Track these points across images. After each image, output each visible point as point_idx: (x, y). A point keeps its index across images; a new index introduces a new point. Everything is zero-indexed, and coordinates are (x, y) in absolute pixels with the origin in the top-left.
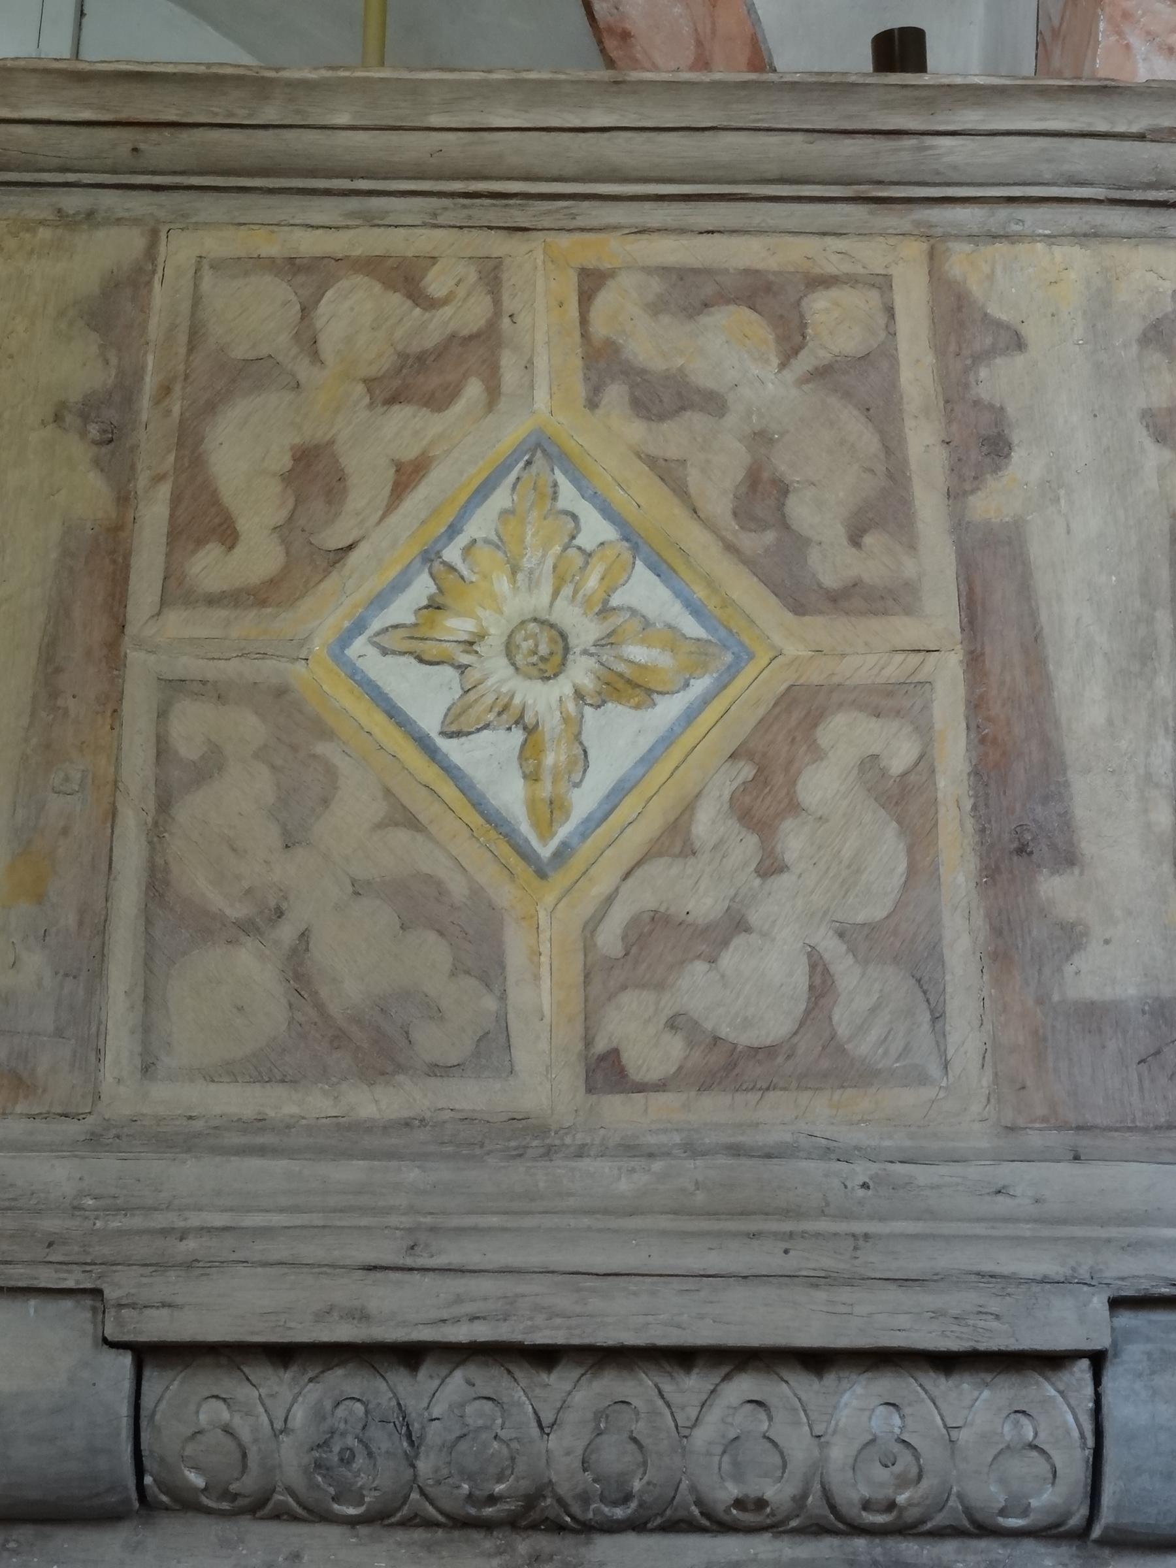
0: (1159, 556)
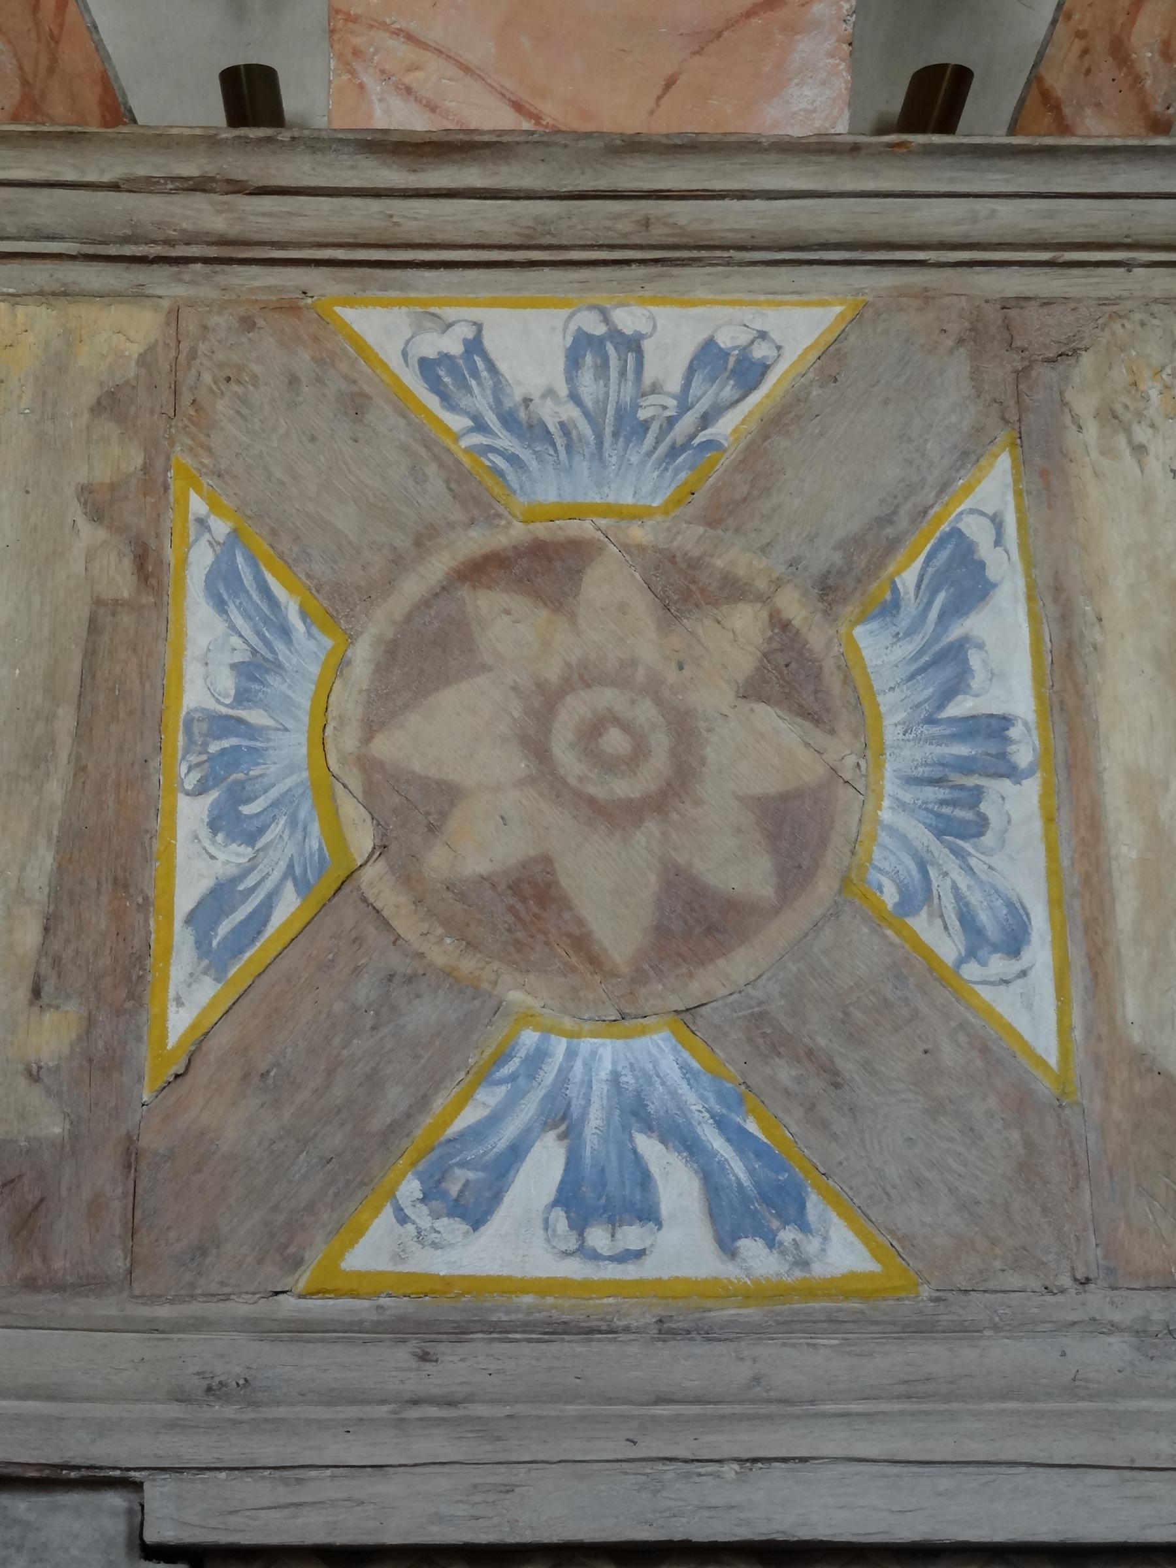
0: (73, 647)
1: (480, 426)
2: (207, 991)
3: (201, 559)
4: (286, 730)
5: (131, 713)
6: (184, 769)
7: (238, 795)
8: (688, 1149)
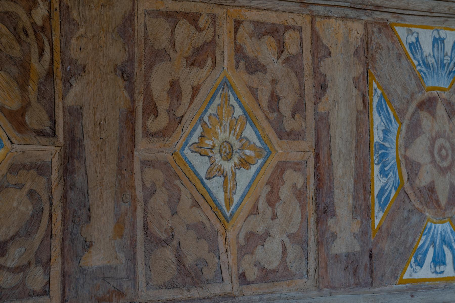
1: (419, 65)
2: (381, 215)
3: (376, 100)
4: (392, 148)
5: (364, 142)
6: (375, 158)
7: (384, 165)
8: (451, 248)
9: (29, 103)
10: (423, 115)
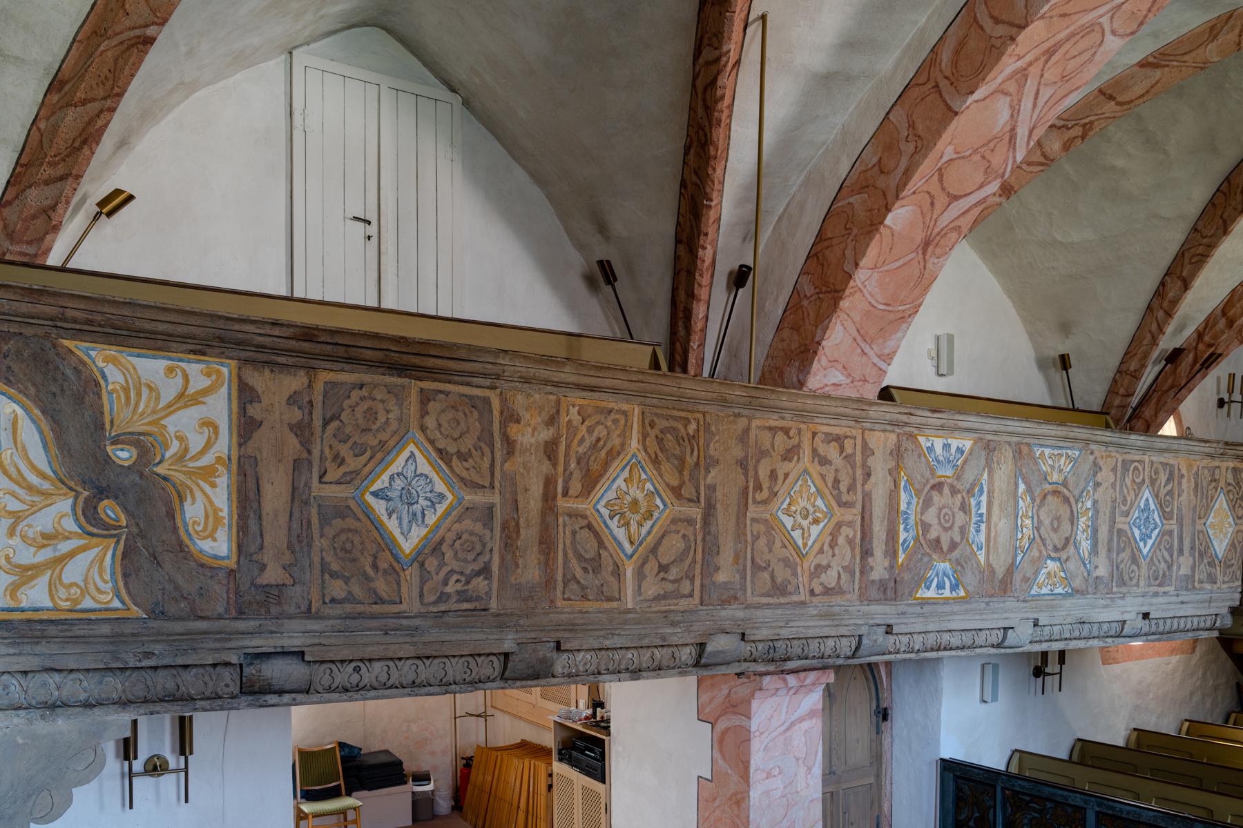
3: (903, 484)
7: (907, 525)
9: (684, 482)
10: (935, 493)
